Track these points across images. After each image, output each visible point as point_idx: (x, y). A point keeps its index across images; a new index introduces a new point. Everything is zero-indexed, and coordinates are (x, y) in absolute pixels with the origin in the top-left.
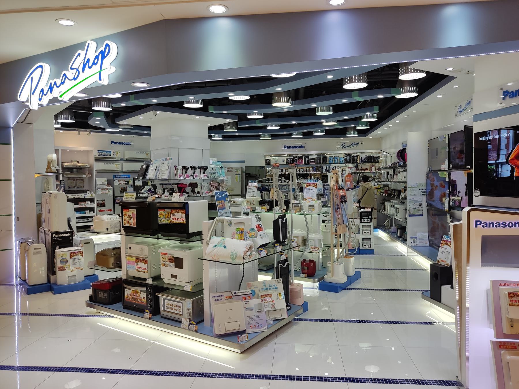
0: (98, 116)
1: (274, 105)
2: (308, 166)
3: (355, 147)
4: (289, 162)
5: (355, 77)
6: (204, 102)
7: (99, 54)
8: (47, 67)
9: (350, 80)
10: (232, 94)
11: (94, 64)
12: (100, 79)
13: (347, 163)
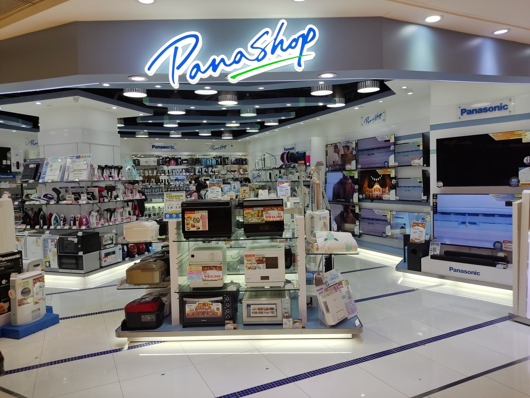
3: (223, 149)
4: (161, 163)
7: (299, 37)
12: (299, 65)
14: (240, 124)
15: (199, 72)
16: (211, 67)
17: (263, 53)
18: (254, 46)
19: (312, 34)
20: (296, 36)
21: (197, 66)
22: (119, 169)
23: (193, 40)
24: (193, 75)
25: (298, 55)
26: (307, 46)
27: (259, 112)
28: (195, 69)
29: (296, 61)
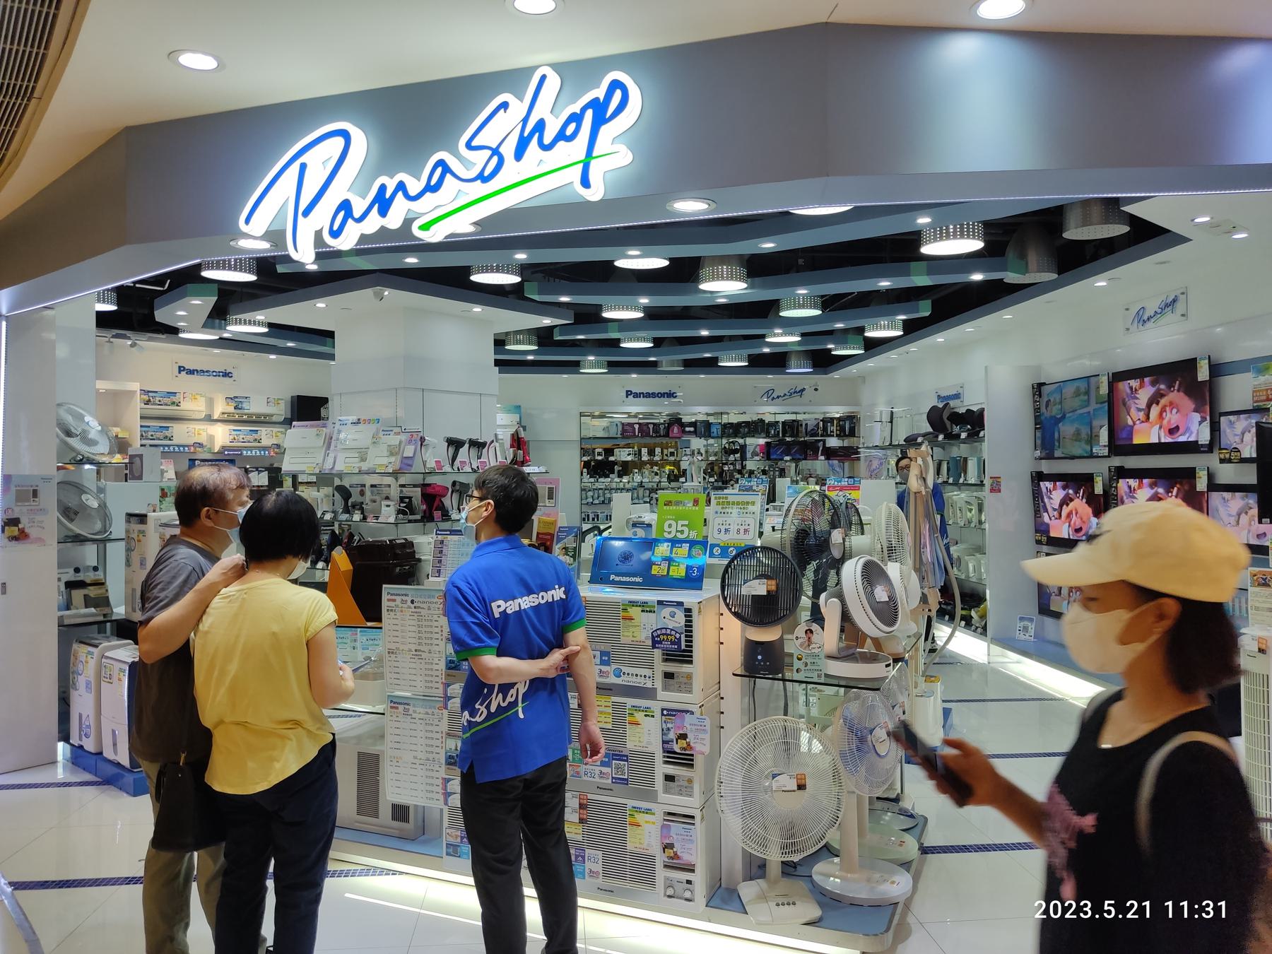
0: (197, 294)
1: (703, 286)
2: (647, 440)
3: (796, 398)
5: (955, 228)
6: (524, 269)
7: (584, 110)
8: (360, 140)
9: (941, 233)
10: (637, 253)
11: (561, 136)
12: (585, 182)
13: (845, 436)
14: (803, 335)
15: (350, 220)
16: (376, 206)
17: (495, 159)
18: (473, 144)
19: (618, 95)
20: (576, 108)
21: (345, 206)
22: (478, 445)
23: (339, 142)
24: (335, 228)
25: (582, 156)
26: (607, 131)
27: (830, 304)
28: (342, 213)
29: (575, 174)
